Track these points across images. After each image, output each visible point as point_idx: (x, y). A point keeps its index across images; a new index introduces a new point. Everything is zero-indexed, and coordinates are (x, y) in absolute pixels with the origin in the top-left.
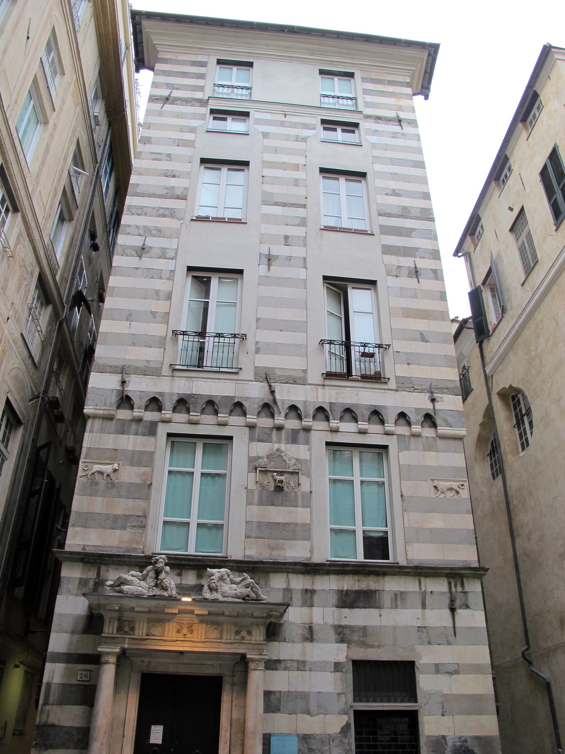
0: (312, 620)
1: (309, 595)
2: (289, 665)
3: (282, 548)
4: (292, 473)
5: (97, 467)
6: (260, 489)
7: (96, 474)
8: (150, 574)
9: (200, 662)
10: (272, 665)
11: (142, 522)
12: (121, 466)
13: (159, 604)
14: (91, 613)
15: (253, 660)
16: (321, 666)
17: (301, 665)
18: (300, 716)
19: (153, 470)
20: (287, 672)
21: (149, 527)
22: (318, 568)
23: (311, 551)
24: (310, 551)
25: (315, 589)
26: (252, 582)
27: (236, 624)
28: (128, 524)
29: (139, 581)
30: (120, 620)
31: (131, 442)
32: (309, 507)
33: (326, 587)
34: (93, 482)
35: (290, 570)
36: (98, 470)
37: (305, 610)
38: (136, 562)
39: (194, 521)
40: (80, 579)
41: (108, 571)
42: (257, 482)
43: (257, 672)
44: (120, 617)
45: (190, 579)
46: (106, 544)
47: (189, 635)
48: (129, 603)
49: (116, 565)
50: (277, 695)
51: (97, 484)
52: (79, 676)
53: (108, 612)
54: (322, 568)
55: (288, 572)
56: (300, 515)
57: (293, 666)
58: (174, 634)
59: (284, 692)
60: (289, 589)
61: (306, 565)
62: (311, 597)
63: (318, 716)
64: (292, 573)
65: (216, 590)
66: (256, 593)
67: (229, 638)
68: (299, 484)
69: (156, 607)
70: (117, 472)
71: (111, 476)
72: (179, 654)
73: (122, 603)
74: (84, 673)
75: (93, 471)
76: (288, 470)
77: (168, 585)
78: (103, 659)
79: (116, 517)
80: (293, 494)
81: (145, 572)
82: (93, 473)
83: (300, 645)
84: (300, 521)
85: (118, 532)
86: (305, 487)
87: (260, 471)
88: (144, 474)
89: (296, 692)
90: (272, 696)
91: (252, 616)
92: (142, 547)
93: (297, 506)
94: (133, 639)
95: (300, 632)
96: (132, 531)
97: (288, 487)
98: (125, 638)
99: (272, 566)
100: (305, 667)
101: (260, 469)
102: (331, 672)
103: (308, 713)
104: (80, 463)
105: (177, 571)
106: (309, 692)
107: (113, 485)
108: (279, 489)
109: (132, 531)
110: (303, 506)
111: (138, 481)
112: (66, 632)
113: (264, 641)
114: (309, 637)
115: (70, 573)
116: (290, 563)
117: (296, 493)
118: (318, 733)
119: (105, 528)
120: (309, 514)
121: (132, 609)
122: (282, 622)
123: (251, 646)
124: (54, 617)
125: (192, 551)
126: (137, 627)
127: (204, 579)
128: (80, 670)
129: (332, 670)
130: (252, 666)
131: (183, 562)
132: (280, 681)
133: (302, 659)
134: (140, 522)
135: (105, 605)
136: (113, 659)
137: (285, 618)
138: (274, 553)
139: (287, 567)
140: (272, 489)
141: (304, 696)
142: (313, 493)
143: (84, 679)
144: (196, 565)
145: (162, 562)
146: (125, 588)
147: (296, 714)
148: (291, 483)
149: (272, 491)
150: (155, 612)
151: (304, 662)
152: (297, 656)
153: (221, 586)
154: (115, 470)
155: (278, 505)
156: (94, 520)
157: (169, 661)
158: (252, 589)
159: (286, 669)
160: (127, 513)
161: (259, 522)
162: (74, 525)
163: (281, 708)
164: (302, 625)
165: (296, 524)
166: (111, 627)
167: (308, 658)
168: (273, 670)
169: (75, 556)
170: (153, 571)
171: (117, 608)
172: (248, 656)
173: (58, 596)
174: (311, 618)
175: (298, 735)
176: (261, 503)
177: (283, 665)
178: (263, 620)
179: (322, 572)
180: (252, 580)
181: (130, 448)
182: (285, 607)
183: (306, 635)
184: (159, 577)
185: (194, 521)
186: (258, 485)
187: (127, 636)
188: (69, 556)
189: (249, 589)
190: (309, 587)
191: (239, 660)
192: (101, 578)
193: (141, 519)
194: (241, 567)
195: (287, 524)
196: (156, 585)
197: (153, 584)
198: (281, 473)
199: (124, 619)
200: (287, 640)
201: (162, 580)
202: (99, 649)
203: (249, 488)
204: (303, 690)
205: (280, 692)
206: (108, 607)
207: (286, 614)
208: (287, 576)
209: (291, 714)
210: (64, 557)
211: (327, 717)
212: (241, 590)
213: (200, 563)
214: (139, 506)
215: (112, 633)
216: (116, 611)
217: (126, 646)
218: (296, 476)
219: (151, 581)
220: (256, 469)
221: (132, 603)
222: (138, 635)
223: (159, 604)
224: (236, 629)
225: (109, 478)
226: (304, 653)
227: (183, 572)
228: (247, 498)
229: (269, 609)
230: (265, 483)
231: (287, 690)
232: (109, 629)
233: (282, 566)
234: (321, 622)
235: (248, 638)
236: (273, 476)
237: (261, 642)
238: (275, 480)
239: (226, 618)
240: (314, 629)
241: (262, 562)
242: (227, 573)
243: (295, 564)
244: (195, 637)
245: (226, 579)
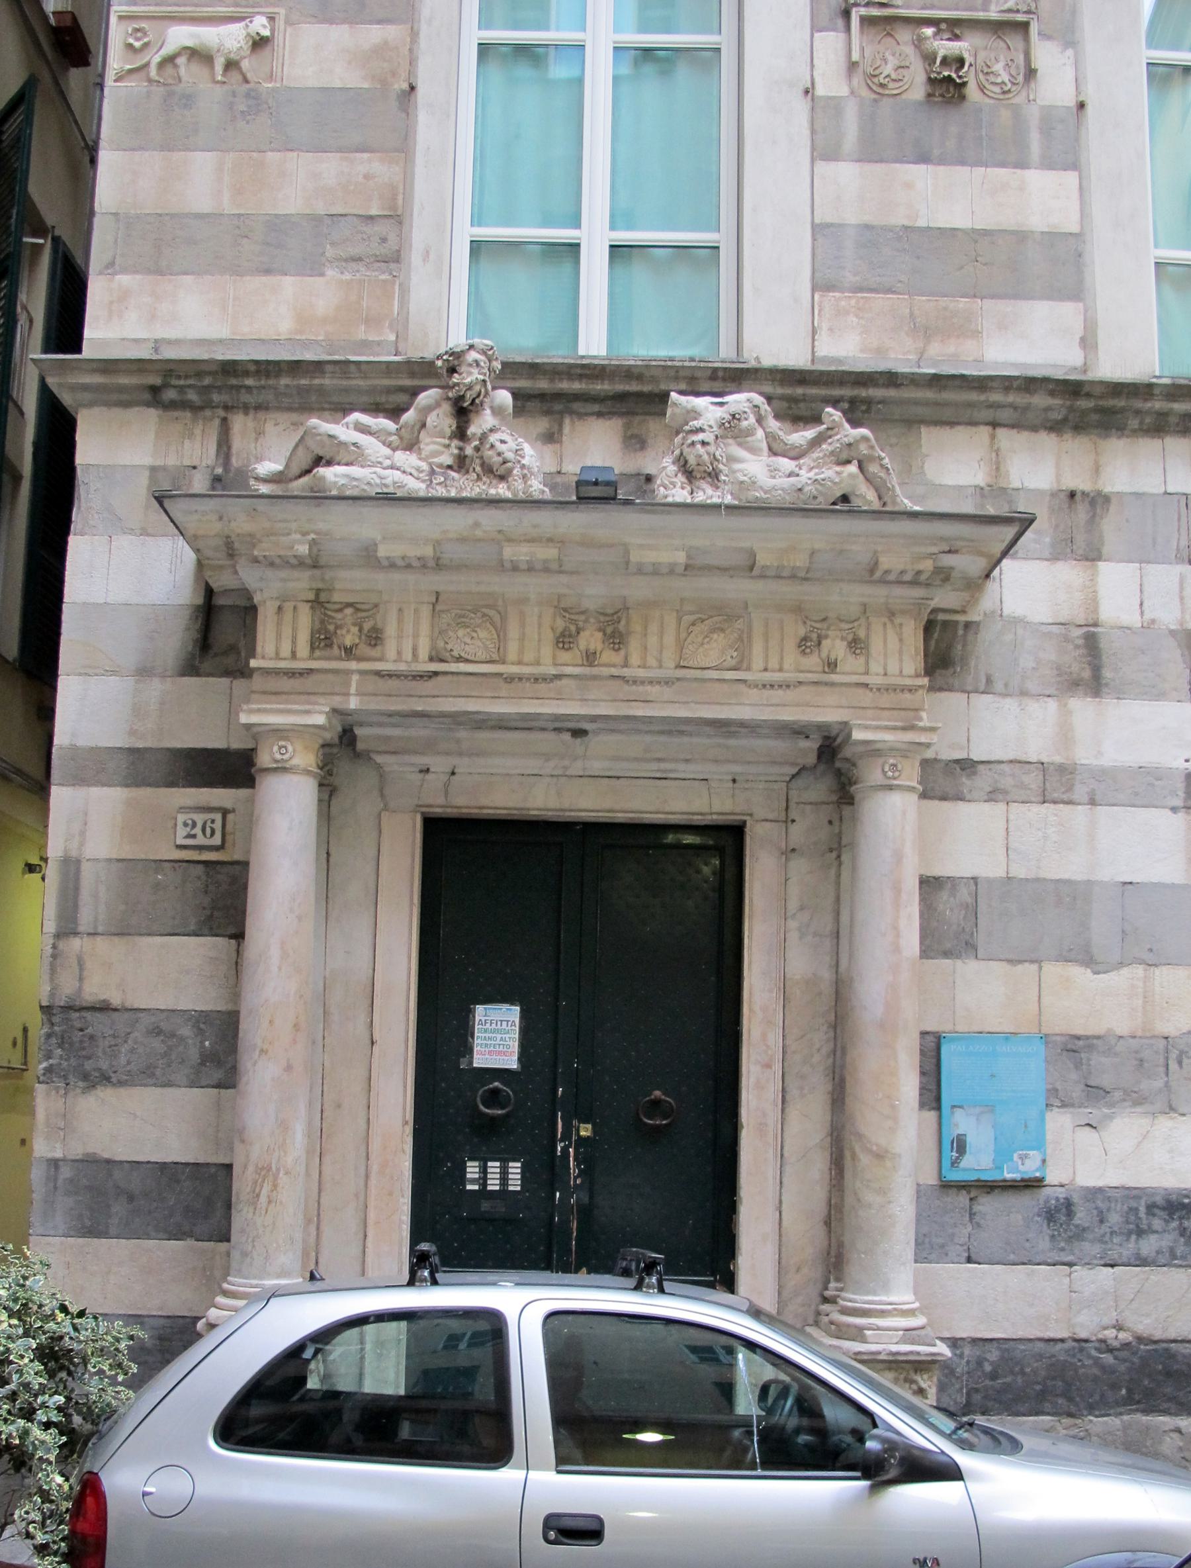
0: (1096, 610)
1: (1082, 511)
2: (1007, 782)
3: (966, 329)
4: (999, 27)
5: (180, 36)
6: (865, 92)
7: (181, 61)
8: (431, 420)
9: (652, 768)
10: (947, 779)
11: (384, 240)
12: (280, 23)
13: (477, 525)
14: (209, 592)
15: (874, 751)
16: (1135, 787)
17: (1056, 782)
18: (1052, 970)
19: (414, 35)
20: (1002, 806)
21: (415, 258)
22: (1120, 403)
23: (1088, 342)
24: (1083, 341)
25: (1107, 489)
26: (865, 439)
27: (798, 609)
28: (330, 252)
29: (388, 451)
30: (318, 602)
32: (1074, 166)
33: (1151, 484)
34: (171, 94)
35: (1005, 415)
36: (190, 44)
37: (1069, 573)
38: (372, 391)
39: (596, 237)
40: (153, 469)
41: (260, 433)
42: (852, 66)
43: (896, 800)
44: (318, 591)
45: (596, 447)
46: (246, 330)
47: (608, 656)
48: (351, 528)
49: (290, 409)
50: (964, 894)
51: (188, 100)
52: (182, 832)
53: (270, 573)
54: (1139, 404)
55: (994, 425)
56: (1040, 199)
57: (1022, 786)
58: (547, 651)
59: (989, 881)
60: (1004, 490)
61: (1071, 389)
62: (1092, 520)
63: (1125, 971)
64: (1015, 426)
65: (713, 476)
66: (881, 491)
67: (773, 663)
68: (1031, 73)
69: (462, 540)
70: (266, 52)
71: (245, 65)
72: (567, 736)
73: (321, 526)
74: (200, 818)
75: (169, 49)
76: (981, 15)
77: (510, 455)
78: (263, 759)
79: (278, 226)
80: (1005, 115)
81: (409, 416)
82: (170, 60)
83: (1052, 705)
84: (1037, 222)
85: (289, 284)
86: (1056, 81)
87: (866, 21)
88: (381, 50)
89: (1037, 880)
90: (944, 895)
91: (872, 573)
92: (393, 338)
93: (1022, 164)
94: (378, 673)
95: (1050, 655)
96: (347, 276)
97: (982, 89)
98: (348, 672)
99: (929, 394)
100: (1070, 789)
101: (863, 11)
102: (1174, 809)
103: (1089, 961)
104: (113, 20)
105: (542, 424)
106: (1089, 883)
107: (256, 102)
108: (947, 88)
109: (347, 276)
110: (1048, 164)
111: (353, 79)
112: (114, 673)
113: (917, 676)
114: (1087, 674)
115: (114, 453)
116: (1008, 383)
117: (1016, 111)
118: (1122, 1028)
119: (237, 271)
120: (1075, 194)
121: (368, 557)
122: (973, 617)
123: (866, 698)
124: (65, 617)
125: (593, 343)
126: (391, 630)
127: (650, 453)
128: (183, 809)
129: (1179, 802)
130: (872, 774)
131: (564, 385)
132: (978, 841)
133: (1058, 759)
134: (378, 239)
135: (252, 540)
136: (304, 757)
137: (987, 601)
138: (935, 349)
139: (996, 397)
140: (918, 92)
141: (1072, 896)
142: (1089, 109)
143: (201, 840)
144: (622, 397)
145: (477, 363)
146: (330, 474)
147: (1038, 961)
148: (998, 67)
149: (920, 103)
150: (460, 567)
151: (1066, 771)
152: (1038, 748)
153: (732, 459)
154: (259, 43)
155: (941, 161)
157: (533, 765)
158: (860, 467)
159: (994, 795)
160: (321, 208)
161: (868, 227)
162: (112, 264)
163: (981, 939)
164: (1055, 629)
165: (1021, 236)
166: (287, 631)
167: (1083, 756)
168: (944, 798)
169: (124, 380)
170: (447, 407)
171: (303, 549)
172: (857, 735)
173: (72, 540)
174: (1093, 603)
175: (1046, 1038)
176: (870, 153)
177: (982, 781)
178: (918, 592)
179: (1134, 423)
180: (863, 431)
182: (1009, 532)
183: (1075, 667)
184: (473, 430)
185: (596, 237)
186: (857, 80)
187: (353, 665)
188: (98, 379)
189: (853, 468)
190: (1082, 484)
191: (811, 759)
192: (235, 462)
193: (379, 228)
194: (804, 399)
195: (985, 233)
196: (461, 463)
197: (447, 459)
198: (954, 27)
199: (337, 597)
200: (999, 686)
201: (483, 438)
202: (244, 719)
203: (820, 91)
204: (1066, 876)
205: (975, 879)
206: (264, 549)
207: (992, 587)
208: (993, 437)
209: (1020, 962)
210: (86, 388)
211: (1162, 975)
212: (814, 474)
213: (634, 387)
214: (367, 177)
215: (294, 655)
216: (301, 563)
217: (353, 703)
218: (1015, 41)
219: (438, 448)
220: (846, 14)
221: (366, 526)
222: (399, 659)
223: (477, 525)
224: (802, 632)
225: (235, 76)
226: (1065, 735)
227: (567, 429)
228: (813, 132)
229: (942, 539)
230: (888, 69)
231: (1000, 873)
232: (278, 641)
233: (973, 396)
234: (1133, 619)
235: (850, 665)
236: (919, 42)
237: (908, 682)
238: (929, 58)
239: (760, 585)
240: (1103, 645)
241: (891, 379)
243: (1030, 384)
244: (635, 659)
245: (750, 432)
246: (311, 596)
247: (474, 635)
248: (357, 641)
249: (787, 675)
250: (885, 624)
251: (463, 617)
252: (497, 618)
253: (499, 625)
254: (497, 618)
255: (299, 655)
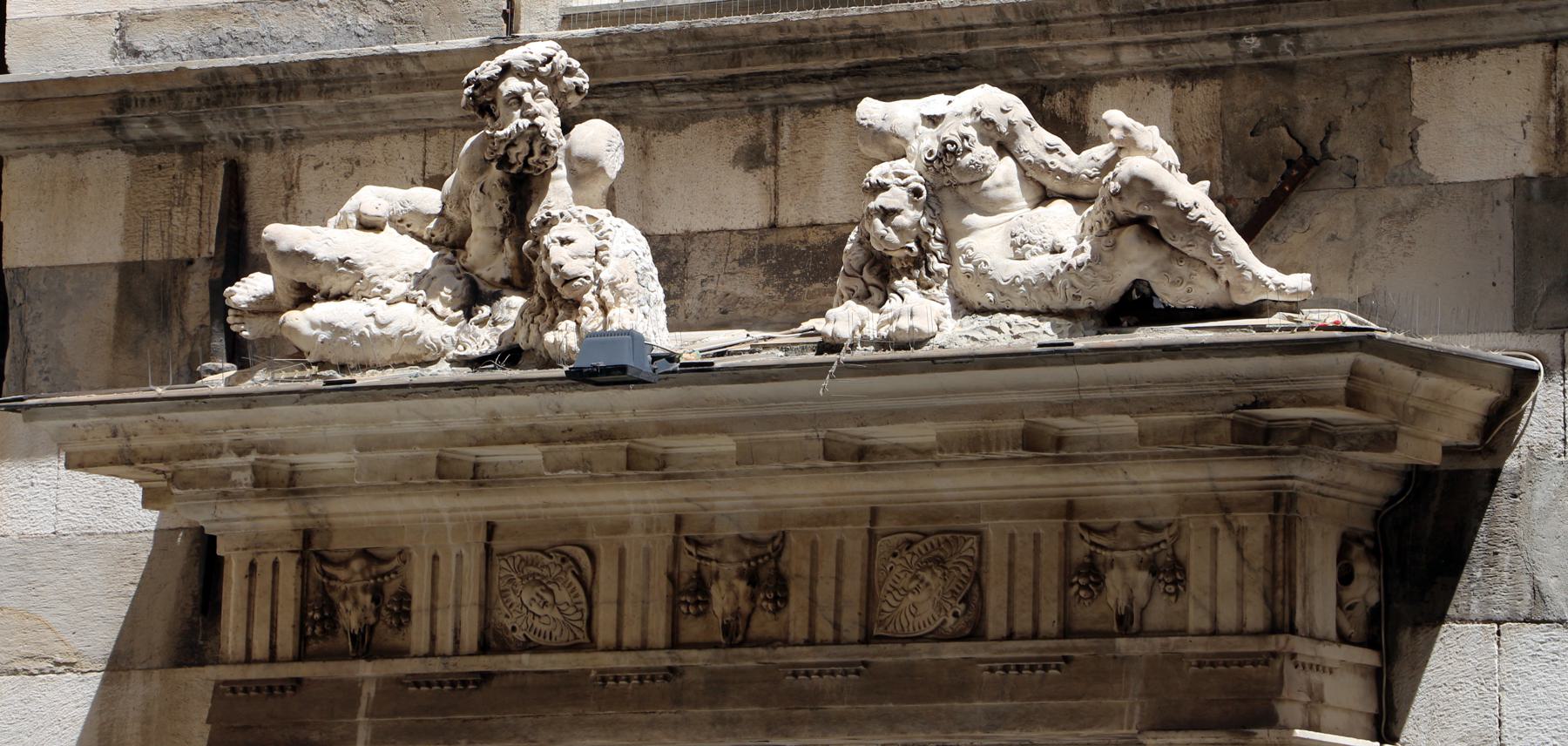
44: (307, 536)
242: (987, 127)
246: (297, 543)
247: (547, 597)
248: (372, 620)
249: (1043, 644)
250: (1215, 531)
251: (533, 563)
252: (584, 560)
253: (588, 573)
254: (584, 560)
255: (280, 652)
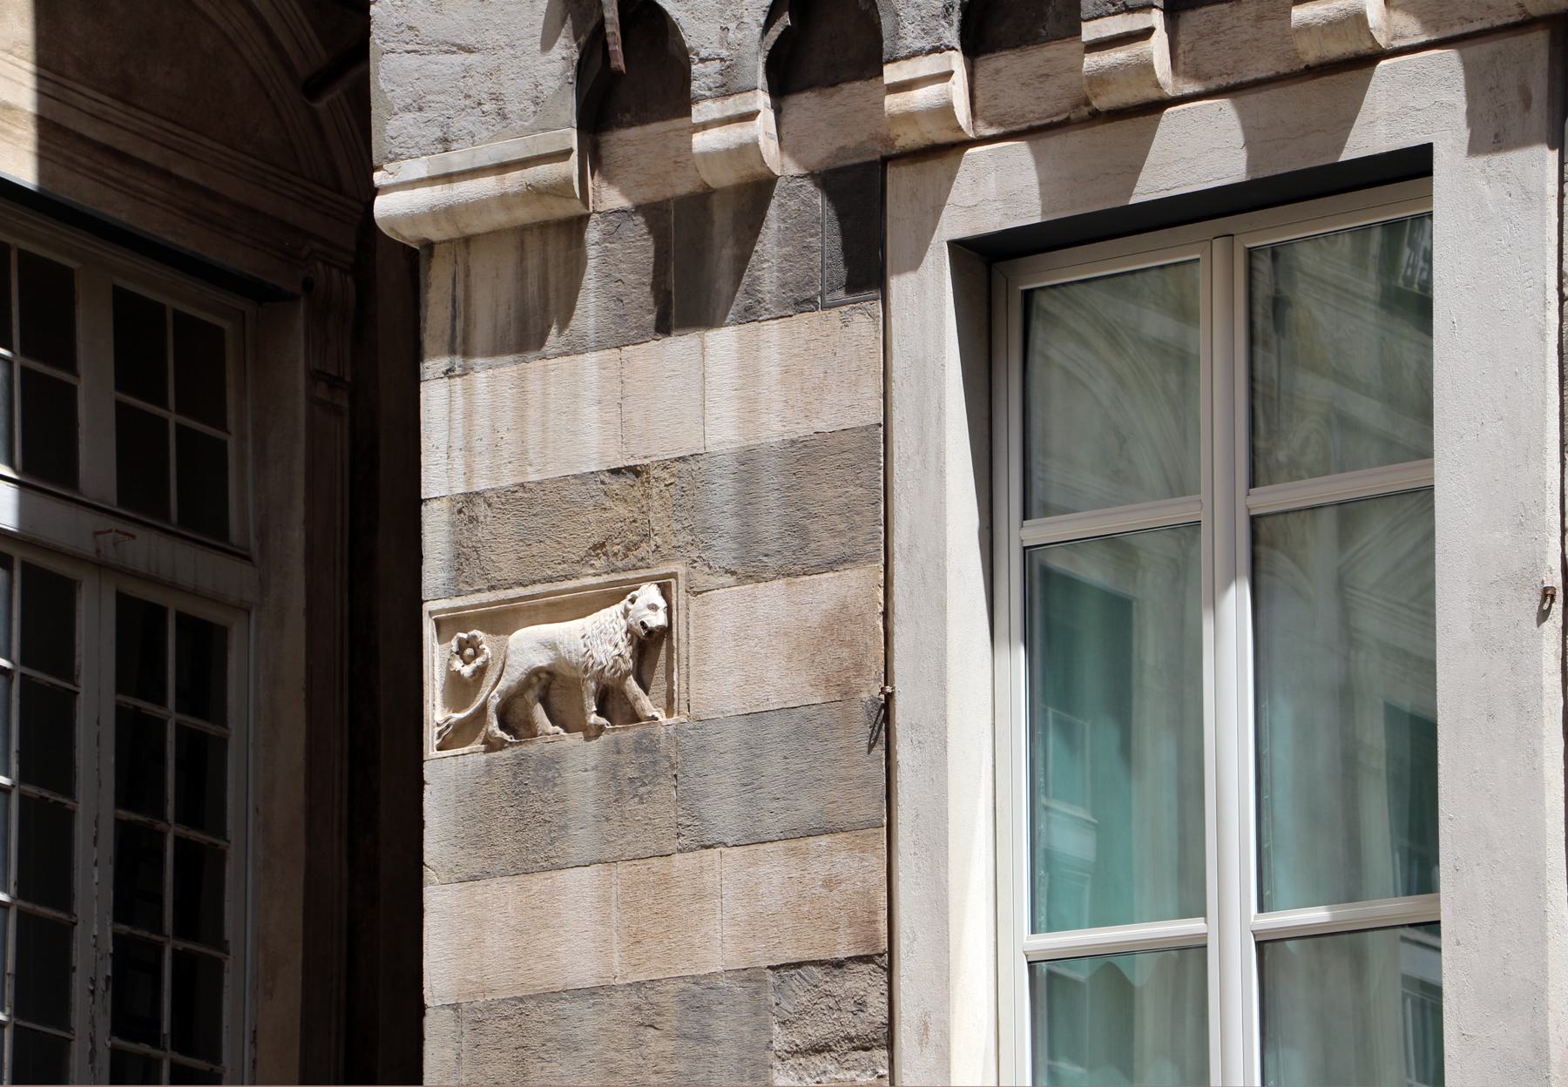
5: (527, 648)
11: (861, 1005)
12: (679, 595)
31: (730, 388)
79: (699, 996)
88: (838, 623)
104: (429, 629)
156: (570, 1046)
181: (722, 433)
214: (829, 884)
